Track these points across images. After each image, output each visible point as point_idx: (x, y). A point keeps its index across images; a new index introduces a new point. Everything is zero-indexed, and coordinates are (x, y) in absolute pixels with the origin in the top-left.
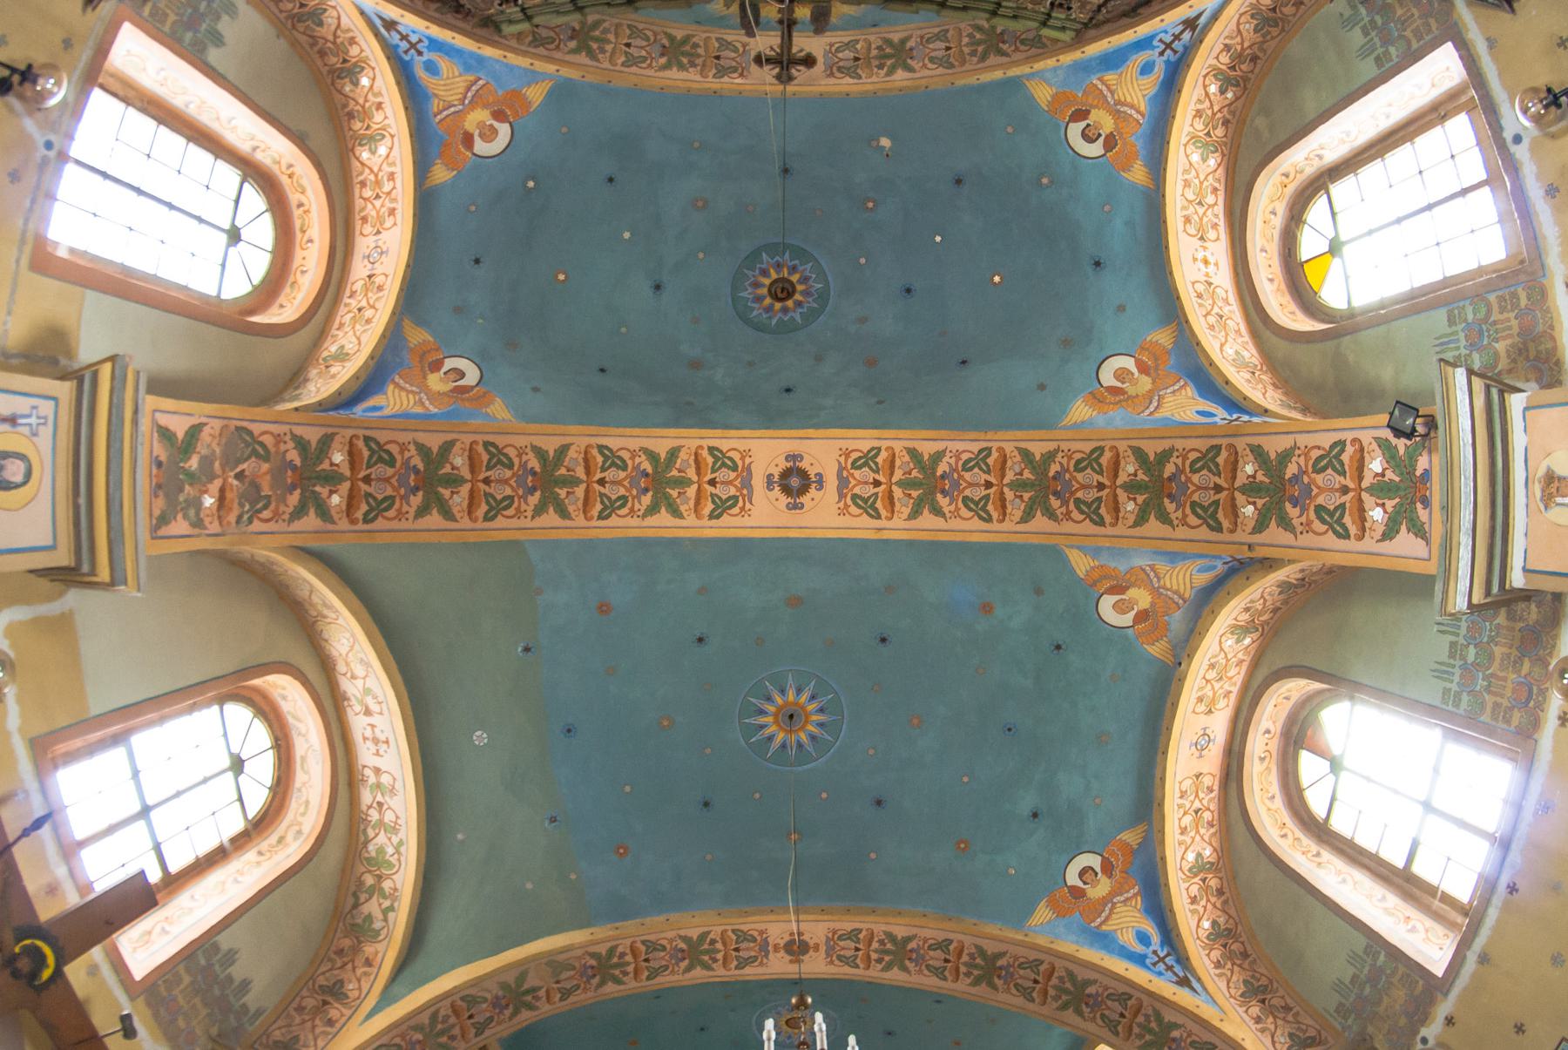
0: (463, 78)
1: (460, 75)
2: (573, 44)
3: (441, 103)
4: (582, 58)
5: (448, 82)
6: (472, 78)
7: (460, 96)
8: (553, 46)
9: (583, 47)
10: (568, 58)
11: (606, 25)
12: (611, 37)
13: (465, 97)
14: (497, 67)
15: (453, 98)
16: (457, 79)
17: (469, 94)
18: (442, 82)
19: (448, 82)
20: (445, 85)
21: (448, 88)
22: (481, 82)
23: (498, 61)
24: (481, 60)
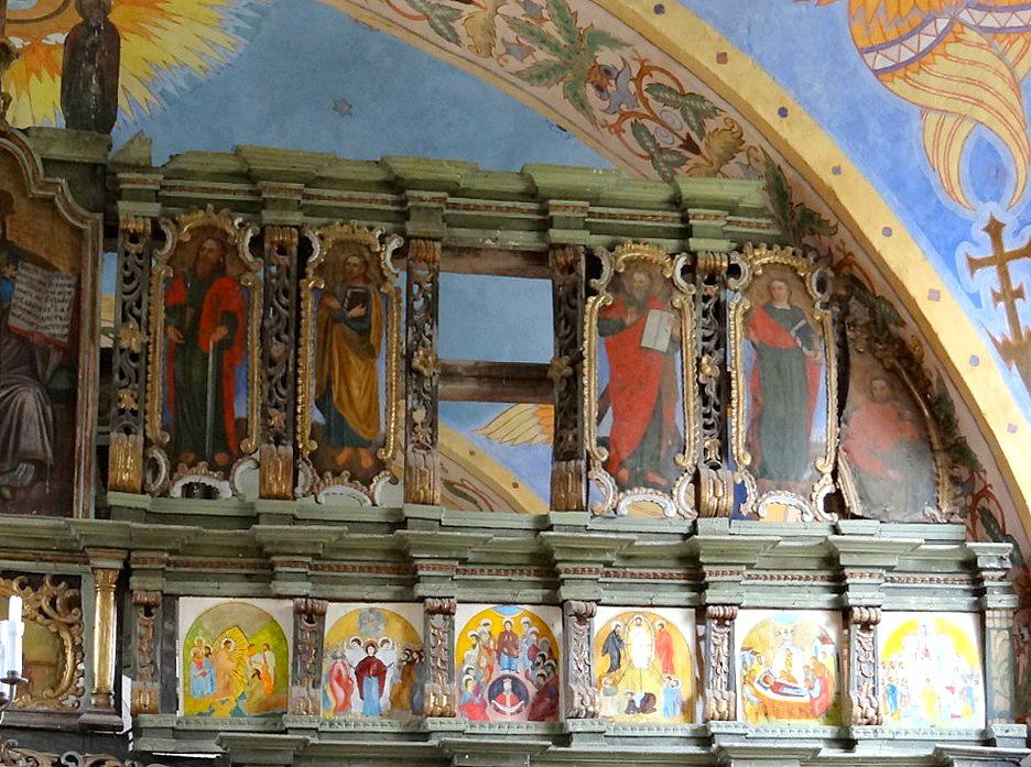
0: (923, 98)
1: (925, 110)
2: (606, 57)
3: (1011, 56)
4: (589, 16)
5: (965, 108)
6: (898, 85)
7: (951, 48)
8: (659, 77)
9: (584, 41)
10: (620, 32)
11: (514, 64)
12: (503, 30)
13: (940, 39)
14: (817, 88)
15: (972, 54)
16: (938, 102)
17: (926, 41)
18: (981, 114)
19: (965, 108)
20: (979, 103)
21: (973, 91)
22: (881, 62)
23: (810, 106)
24: (851, 130)
